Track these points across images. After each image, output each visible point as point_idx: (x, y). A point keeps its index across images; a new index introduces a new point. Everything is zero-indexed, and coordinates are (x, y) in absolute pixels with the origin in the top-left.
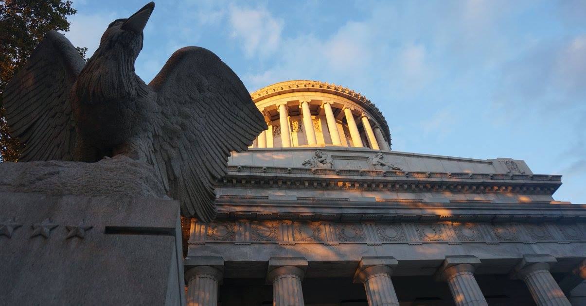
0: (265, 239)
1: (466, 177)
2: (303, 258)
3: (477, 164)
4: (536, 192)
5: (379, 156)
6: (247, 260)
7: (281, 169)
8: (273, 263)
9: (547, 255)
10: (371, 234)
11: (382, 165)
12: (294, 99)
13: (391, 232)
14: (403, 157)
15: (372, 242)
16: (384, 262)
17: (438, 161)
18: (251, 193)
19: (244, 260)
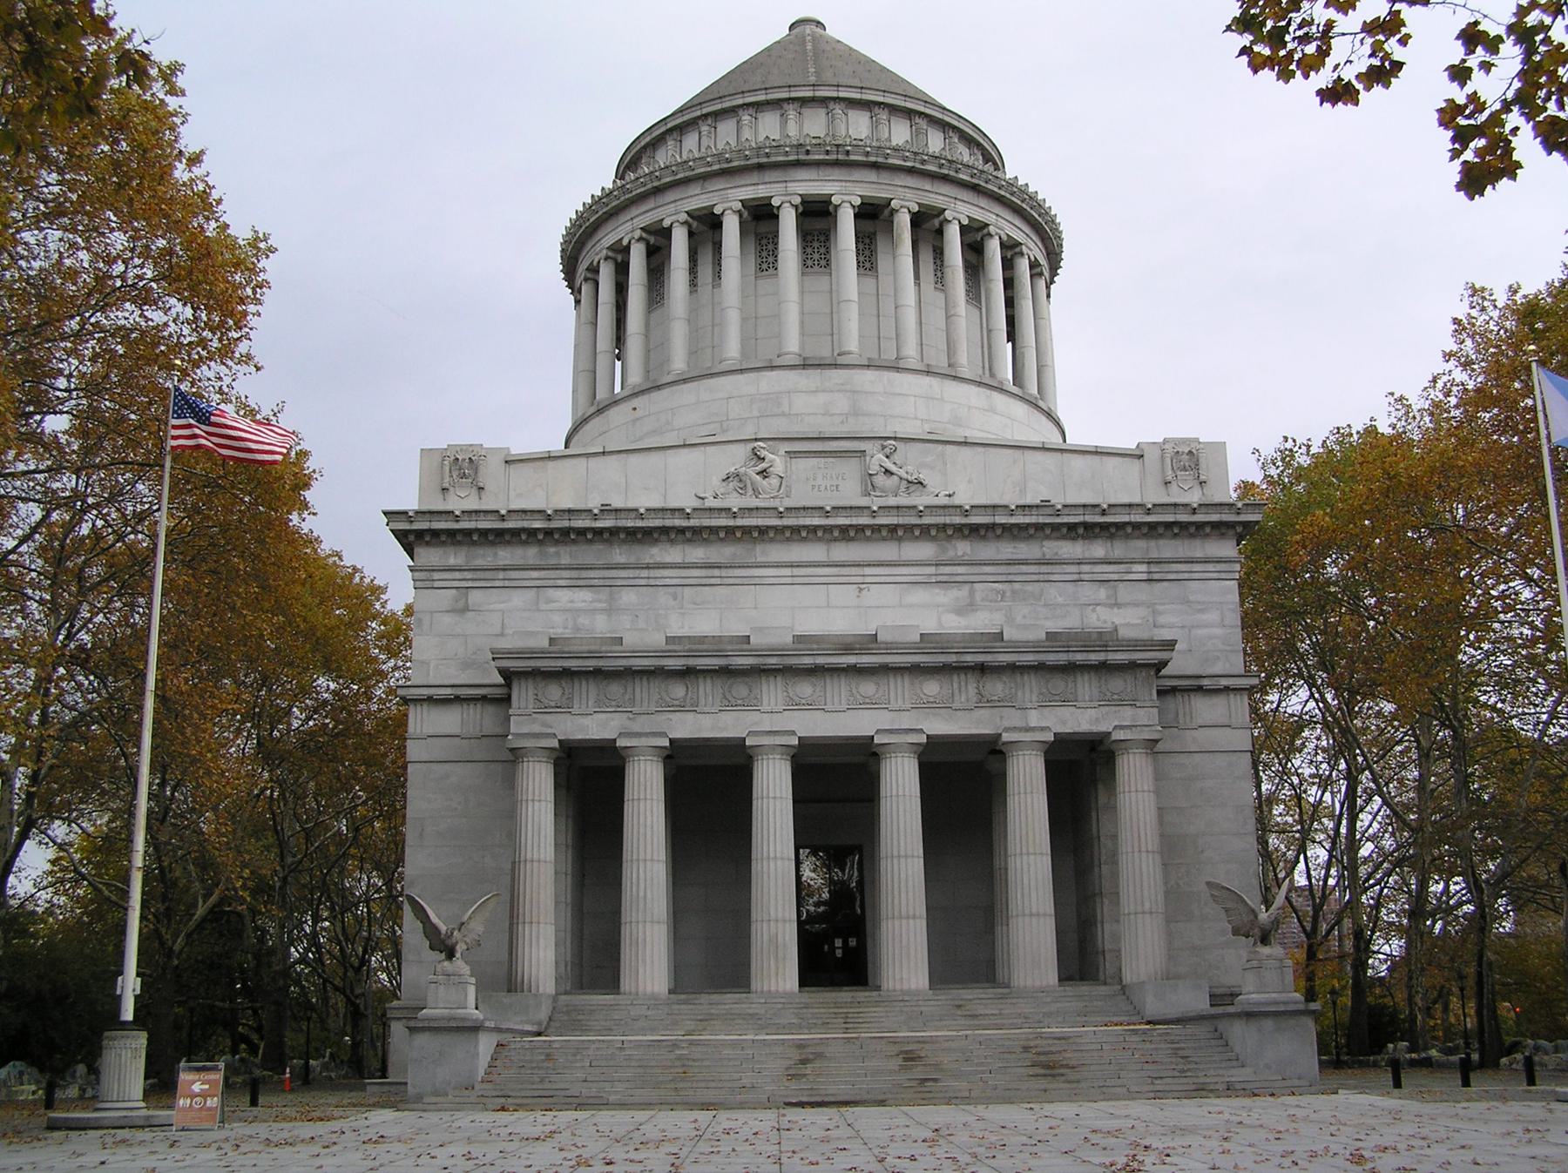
0: (614, 703)
1: (1049, 511)
2: (664, 734)
3: (1105, 458)
4: (1202, 533)
5: (887, 450)
6: (587, 737)
7: (673, 510)
8: (620, 743)
9: (1043, 729)
10: (772, 694)
11: (888, 472)
12: (761, 191)
13: (805, 689)
14: (940, 447)
15: (769, 709)
16: (779, 740)
17: (1018, 453)
18: (620, 554)
19: (583, 737)
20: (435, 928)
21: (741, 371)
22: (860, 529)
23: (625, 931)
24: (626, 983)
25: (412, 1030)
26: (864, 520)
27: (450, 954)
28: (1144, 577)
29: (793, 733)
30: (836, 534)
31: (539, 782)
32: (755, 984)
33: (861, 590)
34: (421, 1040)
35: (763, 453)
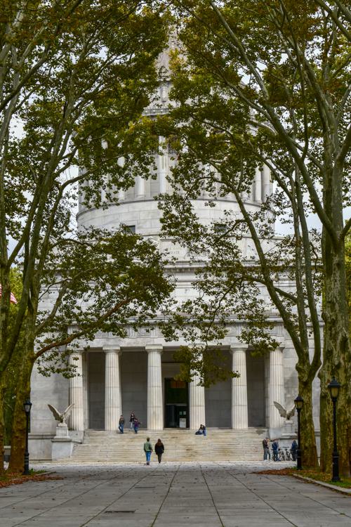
20: (57, 414)
21: (145, 201)
22: (186, 269)
23: (106, 410)
24: (107, 427)
25: (53, 442)
26: (188, 266)
27: (62, 422)
28: (288, 285)
29: (161, 345)
30: (178, 270)
31: (78, 364)
32: (149, 427)
33: (186, 290)
34: (54, 444)
35: (152, 240)
